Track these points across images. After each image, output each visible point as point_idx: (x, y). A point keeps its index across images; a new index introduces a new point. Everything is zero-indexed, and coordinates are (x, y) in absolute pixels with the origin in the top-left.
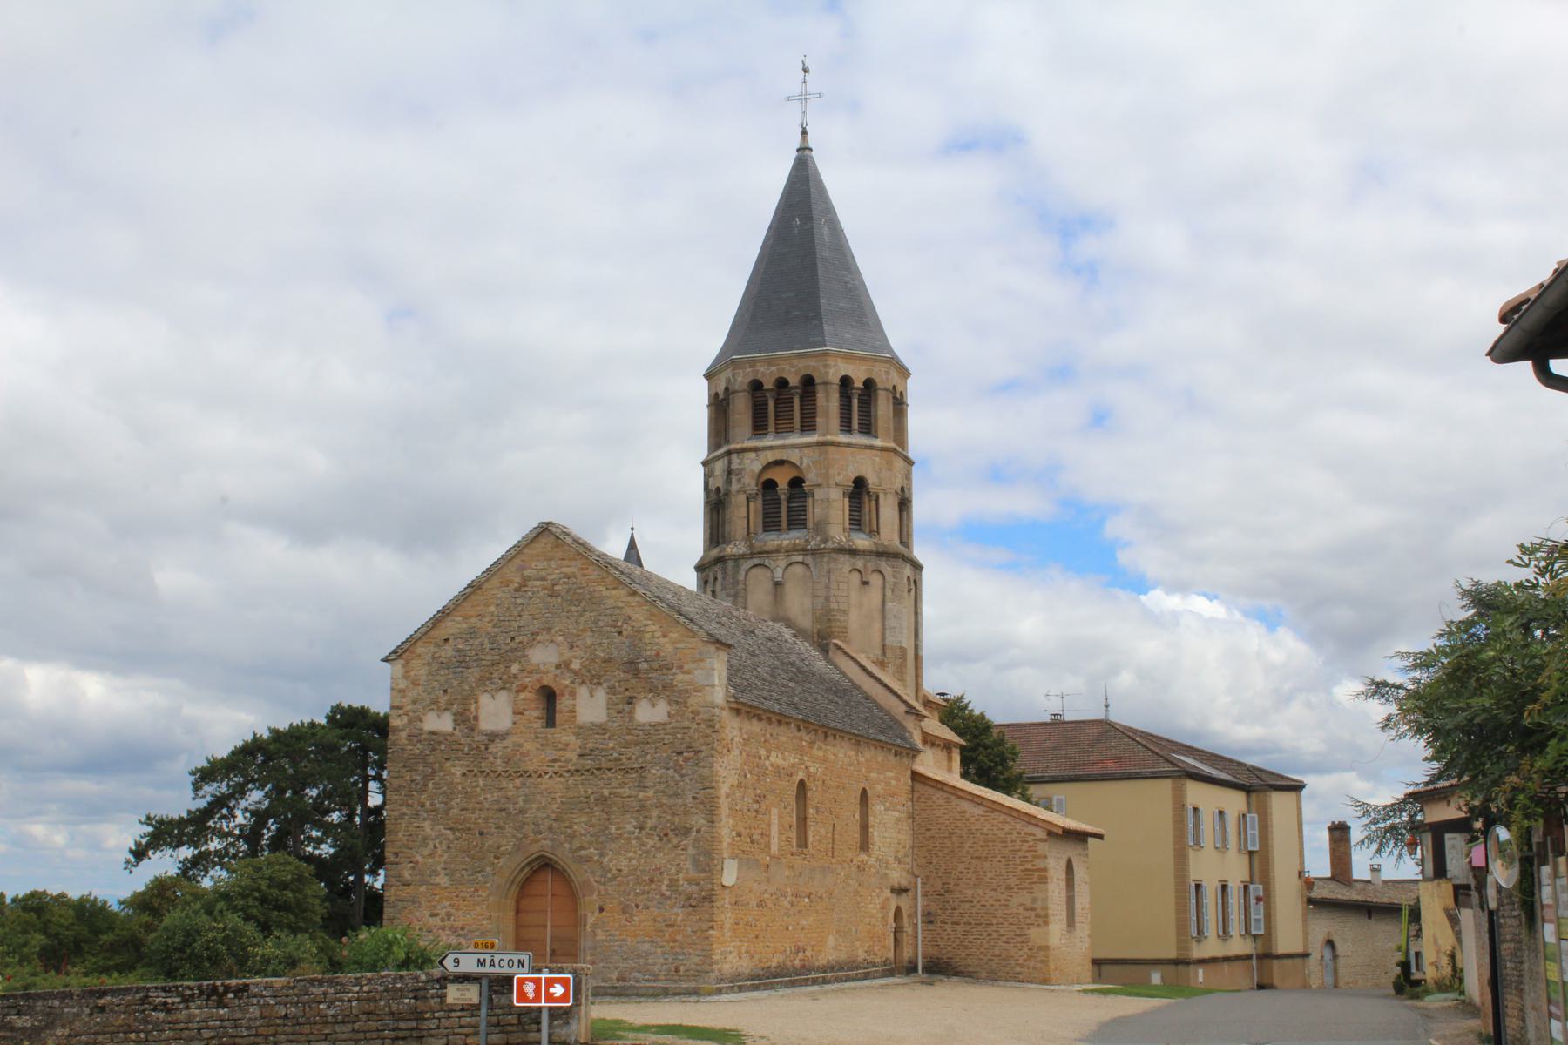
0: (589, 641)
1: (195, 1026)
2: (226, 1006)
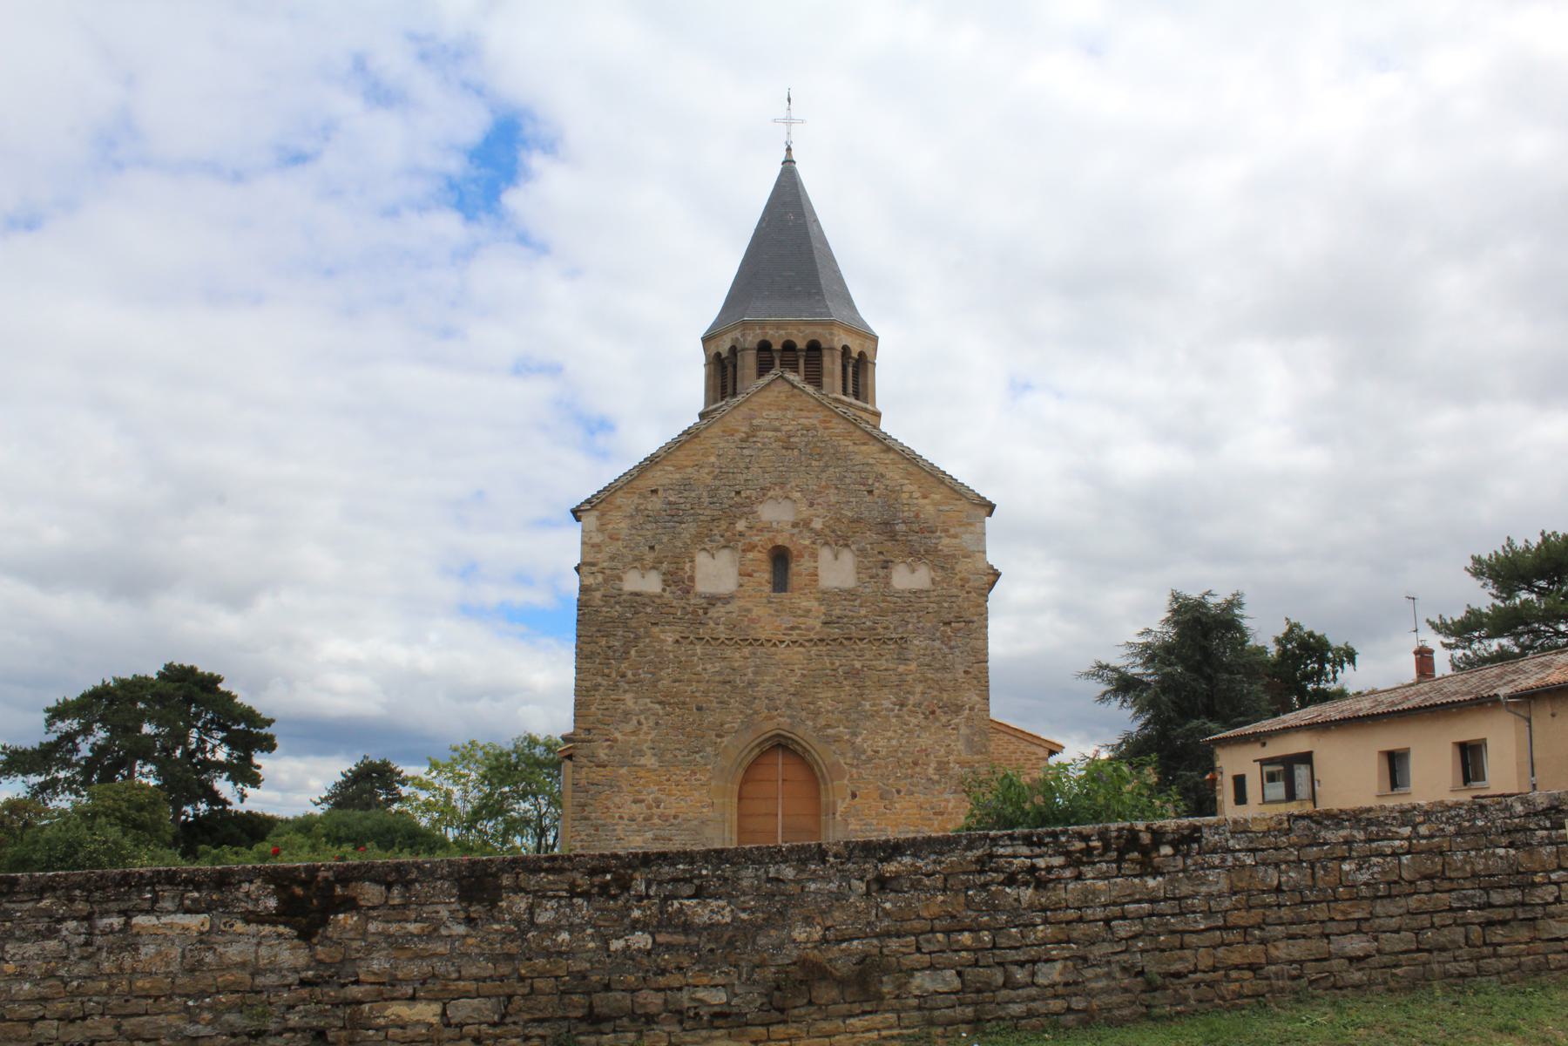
0: (833, 499)
1: (1100, 913)
2: (1156, 872)
